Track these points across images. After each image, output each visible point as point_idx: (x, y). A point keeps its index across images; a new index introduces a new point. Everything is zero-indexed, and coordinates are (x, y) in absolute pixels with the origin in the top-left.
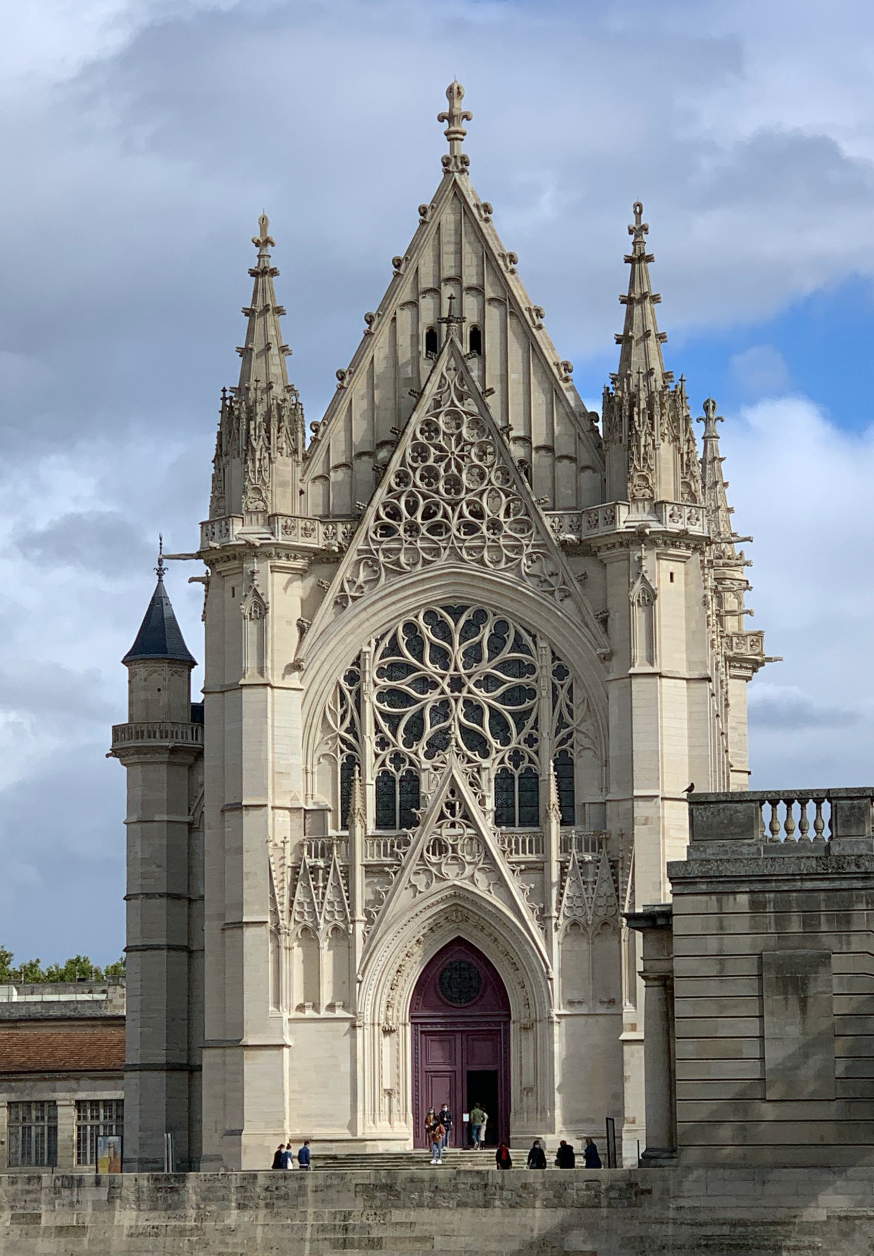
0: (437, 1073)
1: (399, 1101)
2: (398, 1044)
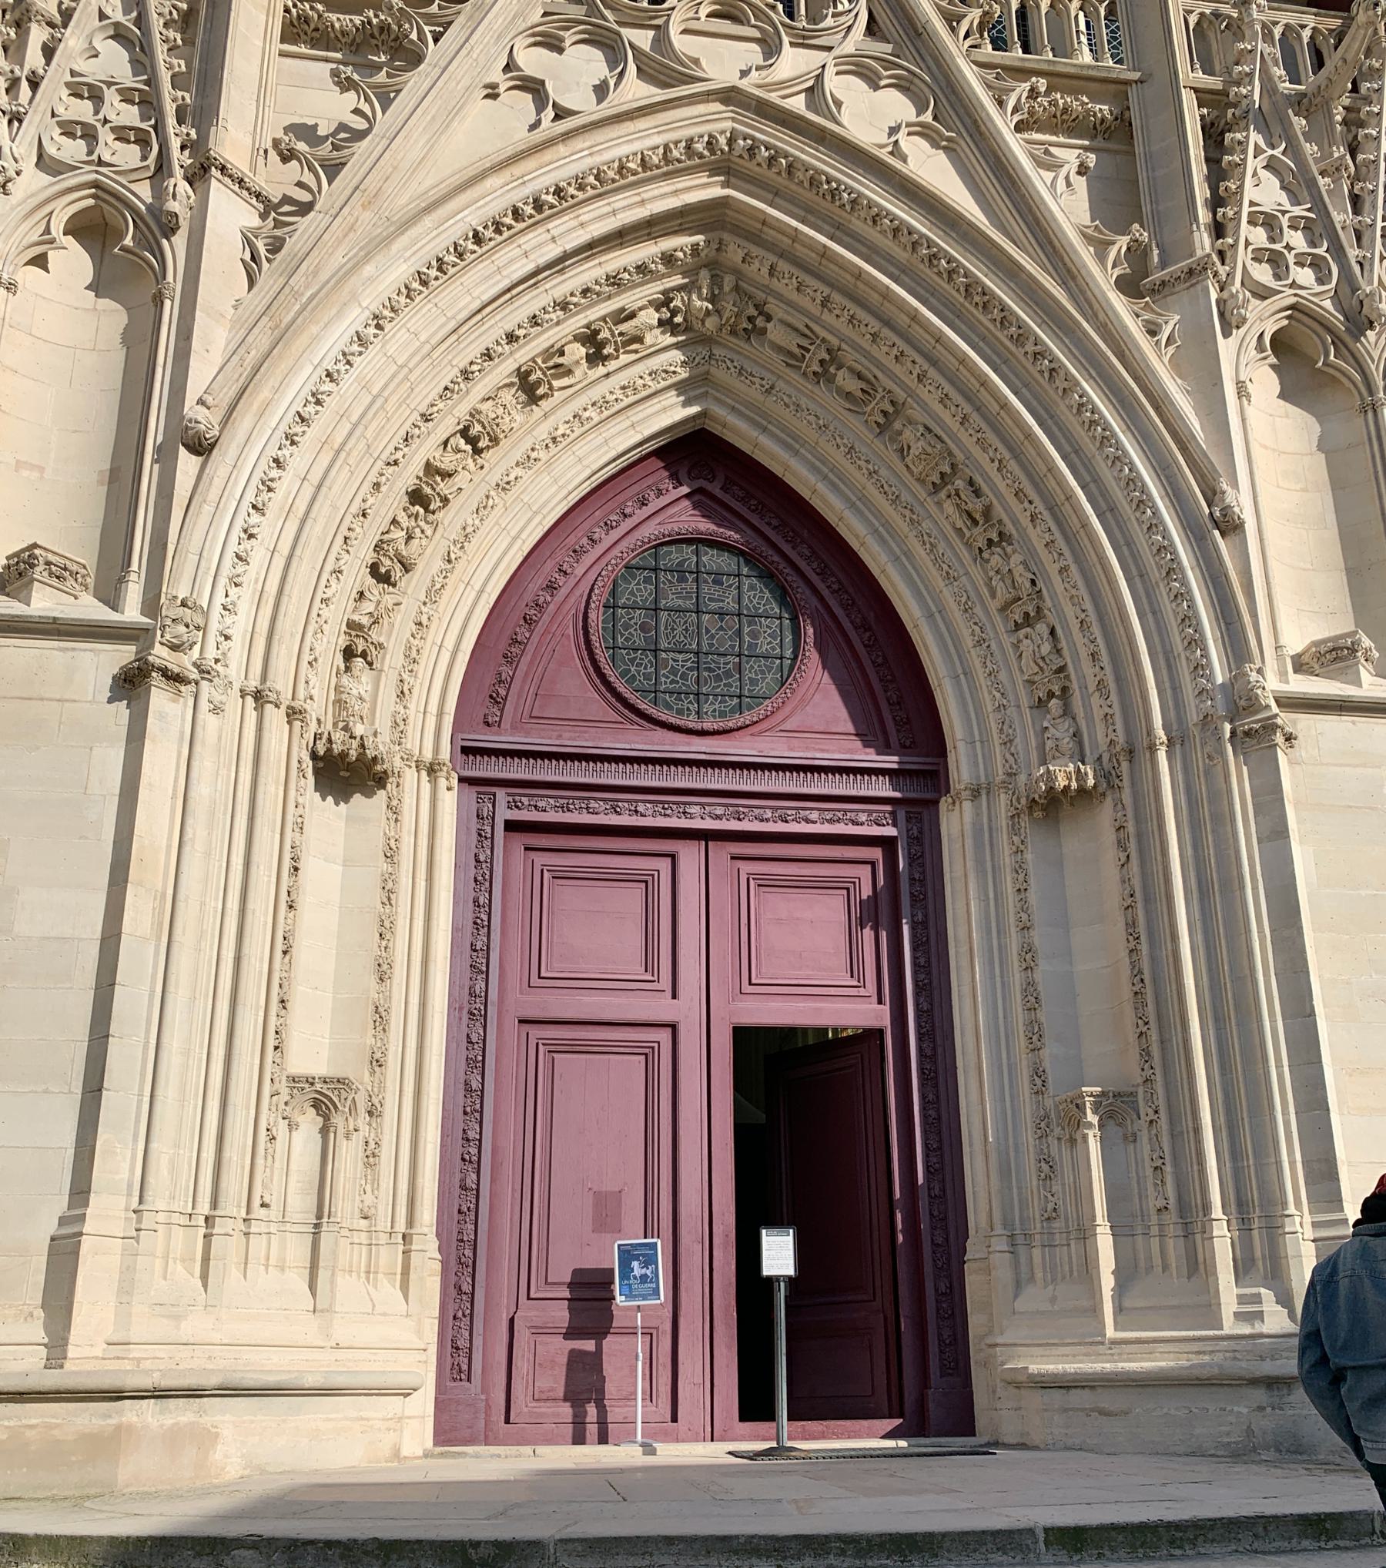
0: (585, 1035)
1: (371, 1157)
2: (390, 855)
